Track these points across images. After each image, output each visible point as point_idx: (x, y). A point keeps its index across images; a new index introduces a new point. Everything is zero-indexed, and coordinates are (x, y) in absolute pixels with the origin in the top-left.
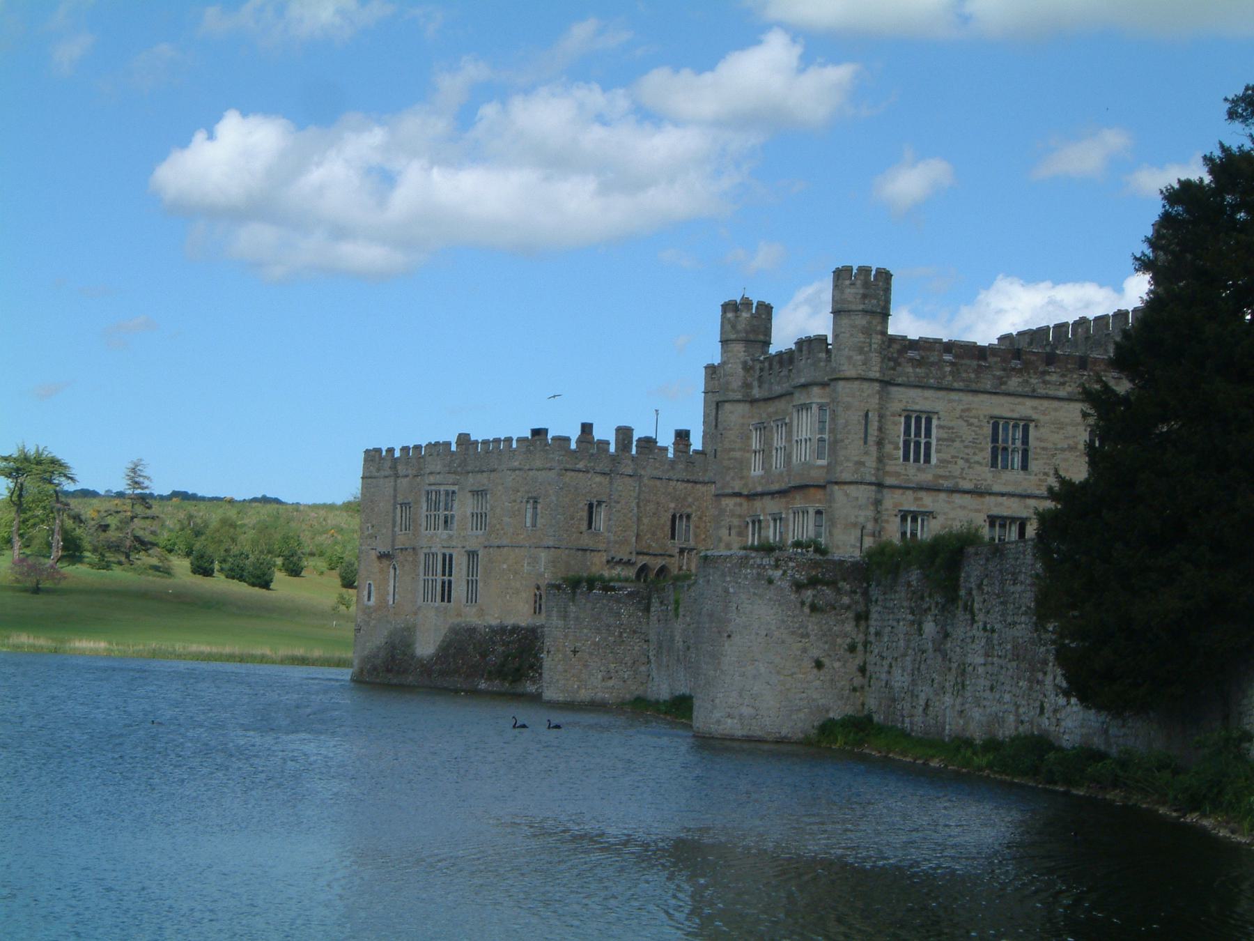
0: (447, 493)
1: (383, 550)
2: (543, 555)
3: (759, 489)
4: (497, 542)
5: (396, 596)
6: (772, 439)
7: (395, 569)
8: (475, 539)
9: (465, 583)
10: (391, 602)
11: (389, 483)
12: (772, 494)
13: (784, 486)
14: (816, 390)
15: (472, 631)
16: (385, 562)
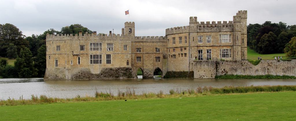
0: (100, 43)
1: (75, 53)
2: (129, 55)
3: (202, 45)
4: (117, 53)
5: (80, 63)
6: (206, 38)
7: (79, 58)
8: (109, 53)
9: (106, 60)
10: (78, 64)
11: (79, 41)
12: (207, 46)
13: (211, 45)
14: (229, 32)
15: (111, 69)
16: (75, 57)
